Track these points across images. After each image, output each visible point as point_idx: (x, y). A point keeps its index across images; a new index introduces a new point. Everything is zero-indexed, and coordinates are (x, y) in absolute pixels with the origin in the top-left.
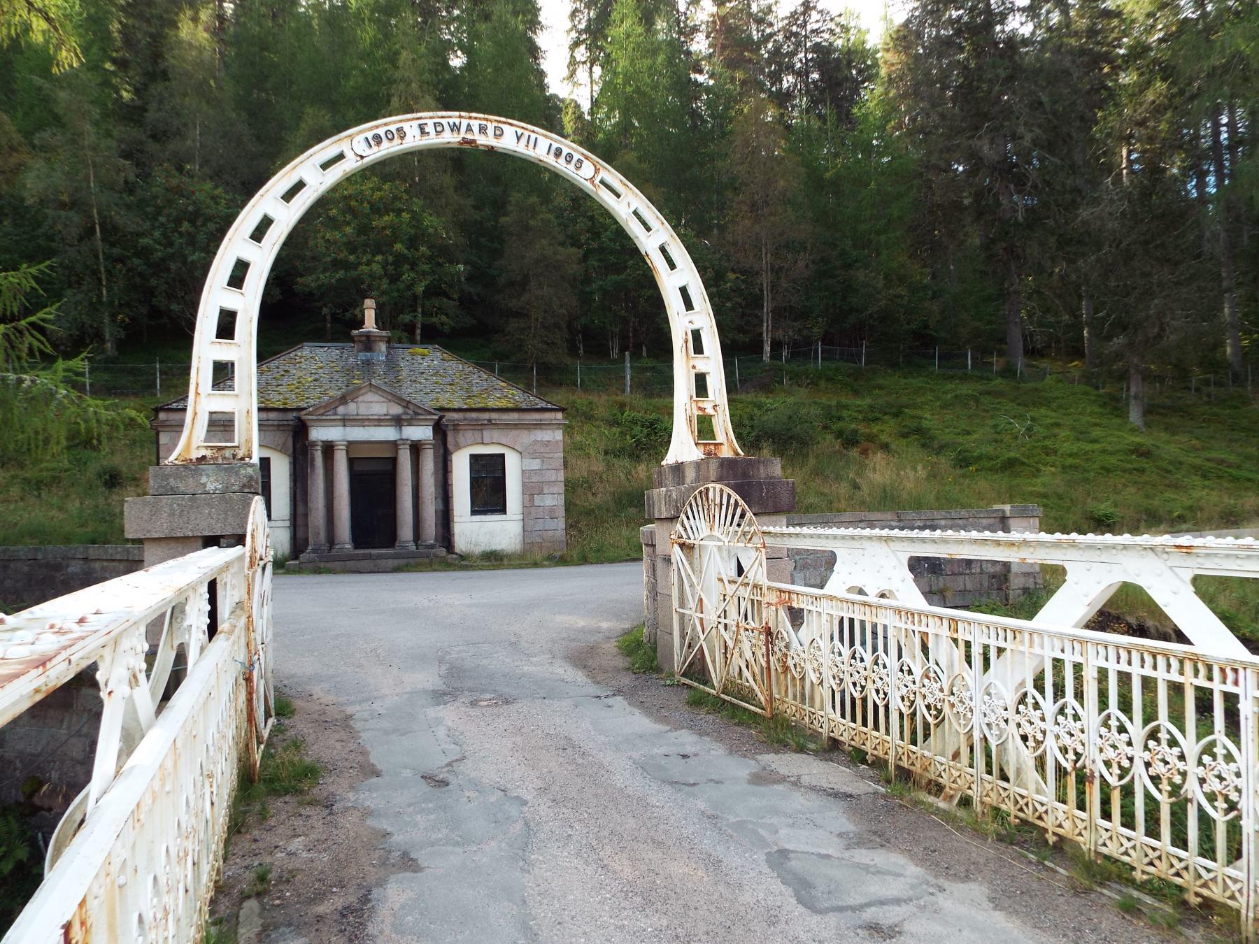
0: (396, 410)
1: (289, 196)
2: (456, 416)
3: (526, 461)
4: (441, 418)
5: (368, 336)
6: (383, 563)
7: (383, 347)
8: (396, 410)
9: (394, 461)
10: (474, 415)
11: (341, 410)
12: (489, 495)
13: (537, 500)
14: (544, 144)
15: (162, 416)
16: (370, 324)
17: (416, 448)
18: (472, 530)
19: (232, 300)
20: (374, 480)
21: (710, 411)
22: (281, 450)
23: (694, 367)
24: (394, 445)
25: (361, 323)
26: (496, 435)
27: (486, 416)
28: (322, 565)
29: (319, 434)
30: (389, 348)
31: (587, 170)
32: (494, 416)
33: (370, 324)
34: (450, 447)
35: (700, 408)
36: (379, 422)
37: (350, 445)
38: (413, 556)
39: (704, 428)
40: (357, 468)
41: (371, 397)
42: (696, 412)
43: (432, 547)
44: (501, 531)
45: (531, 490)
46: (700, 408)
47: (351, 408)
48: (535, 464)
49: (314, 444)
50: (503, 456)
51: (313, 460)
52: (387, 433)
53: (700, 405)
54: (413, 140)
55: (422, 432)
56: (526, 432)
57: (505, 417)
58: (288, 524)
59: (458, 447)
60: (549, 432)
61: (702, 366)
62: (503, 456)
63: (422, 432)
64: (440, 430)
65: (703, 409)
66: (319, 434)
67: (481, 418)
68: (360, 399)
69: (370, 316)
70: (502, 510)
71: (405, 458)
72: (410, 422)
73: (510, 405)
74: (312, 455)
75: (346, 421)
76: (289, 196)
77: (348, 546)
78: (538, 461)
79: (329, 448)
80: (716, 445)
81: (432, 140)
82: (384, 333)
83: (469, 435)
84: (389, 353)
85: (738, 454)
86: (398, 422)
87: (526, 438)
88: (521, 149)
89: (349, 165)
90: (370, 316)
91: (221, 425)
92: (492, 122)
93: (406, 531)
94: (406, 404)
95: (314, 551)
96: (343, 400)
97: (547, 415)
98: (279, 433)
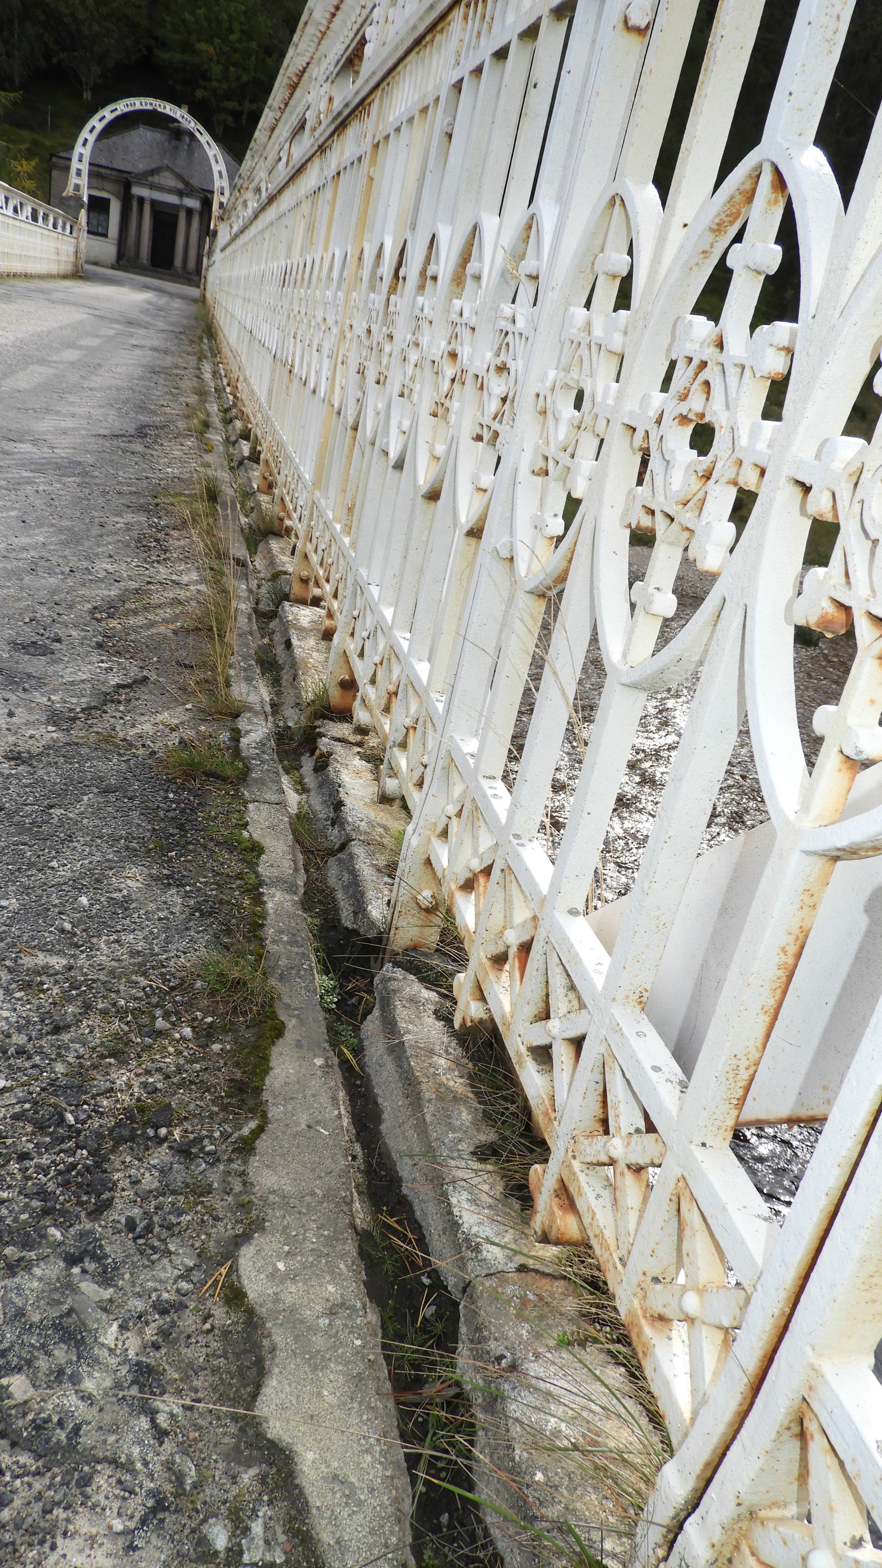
0: (180, 186)
1: (101, 120)
8: (180, 186)
9: (176, 218)
11: (150, 179)
14: (179, 113)
15: (54, 159)
17: (190, 212)
19: (83, 151)
22: (117, 197)
24: (177, 207)
31: (192, 124)
36: (170, 191)
37: (153, 202)
41: (167, 174)
47: (156, 179)
52: (173, 199)
54: (138, 107)
63: (193, 203)
66: (137, 191)
72: (188, 196)
75: (152, 187)
76: (101, 120)
79: (141, 200)
81: (144, 107)
86: (181, 194)
88: (171, 114)
89: (118, 113)
91: (77, 187)
92: (163, 103)
93: (178, 261)
94: (187, 184)
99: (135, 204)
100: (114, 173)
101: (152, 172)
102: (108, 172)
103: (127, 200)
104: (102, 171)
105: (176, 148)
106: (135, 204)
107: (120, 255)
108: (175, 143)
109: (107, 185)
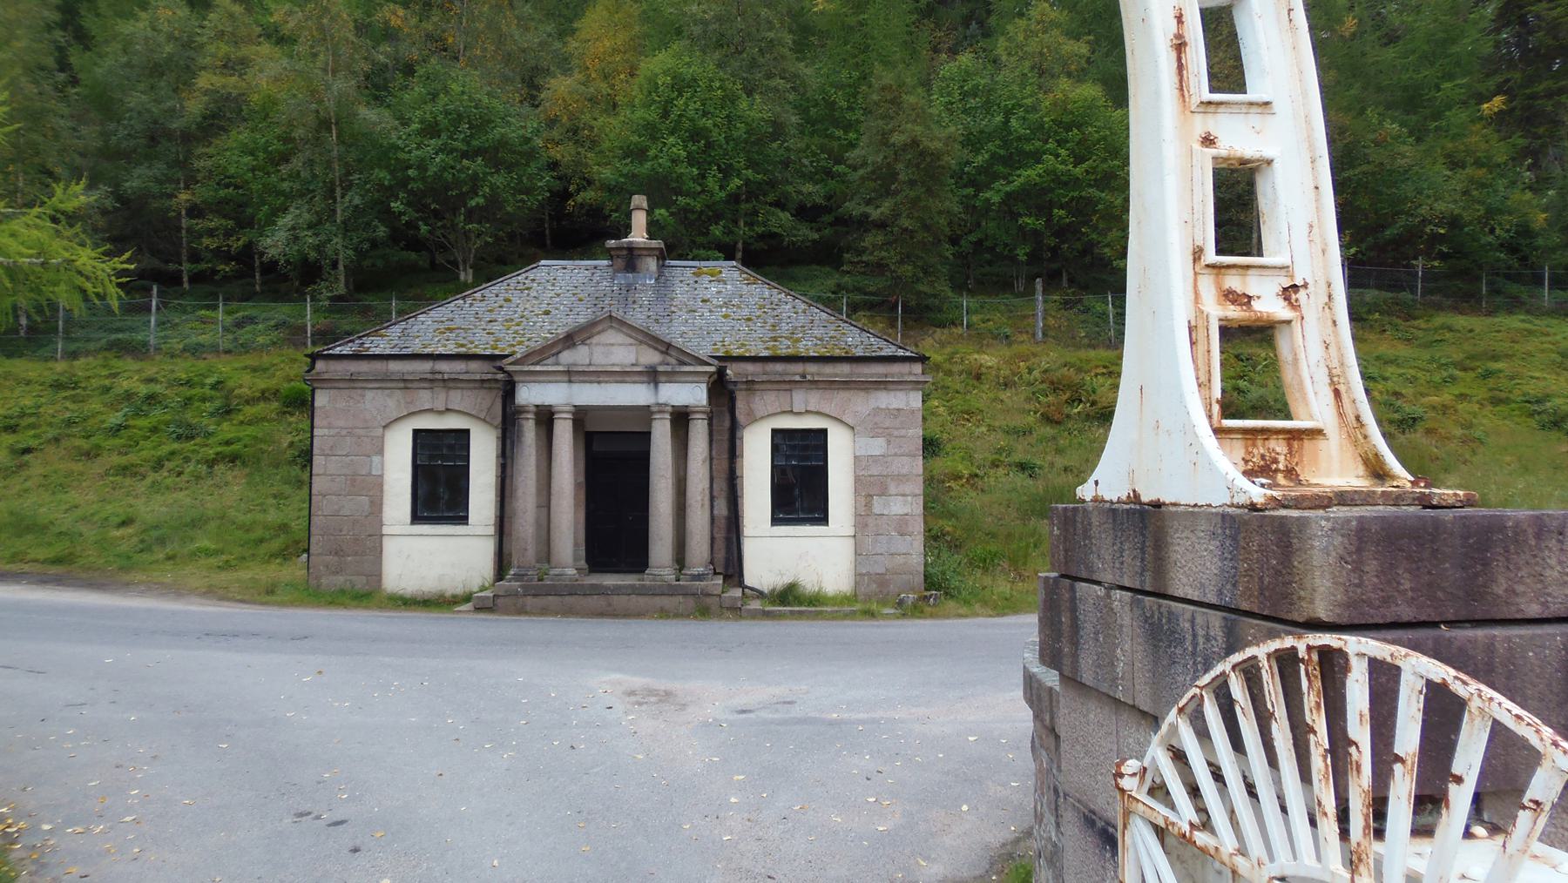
0: (651, 357)
2: (750, 368)
3: (862, 441)
4: (721, 372)
5: (631, 250)
6: (619, 601)
7: (652, 264)
8: (651, 357)
10: (779, 367)
11: (567, 357)
12: (801, 491)
13: (878, 505)
16: (638, 235)
17: (681, 418)
18: (775, 553)
20: (615, 463)
21: (1270, 305)
23: (1208, 141)
24: (645, 413)
25: (627, 229)
26: (814, 399)
27: (798, 368)
28: (529, 600)
29: (530, 395)
30: (661, 267)
32: (812, 368)
33: (638, 235)
34: (741, 416)
35: (1230, 296)
36: (622, 376)
37: (581, 416)
38: (671, 591)
39: (1249, 365)
40: (596, 447)
41: (612, 336)
42: (1217, 311)
43: (699, 577)
44: (815, 556)
45: (868, 487)
46: (1230, 296)
47: (577, 356)
48: (877, 446)
49: (521, 410)
50: (824, 432)
51: (520, 434)
52: (634, 395)
53: (1233, 282)
55: (693, 394)
56: (862, 394)
57: (829, 370)
58: (491, 530)
59: (754, 419)
60: (901, 395)
61: (1239, 138)
62: (824, 432)
63: (693, 394)
64: (722, 390)
65: (1245, 300)
66: (530, 395)
67: (789, 368)
68: (595, 340)
69: (639, 220)
70: (823, 519)
71: (661, 434)
72: (672, 377)
73: (837, 352)
74: (520, 426)
75: (572, 375)
77: (571, 571)
78: (881, 441)
79: (546, 417)
80: (1294, 436)
82: (655, 243)
83: (766, 401)
84: (660, 274)
85: (1378, 471)
86: (653, 376)
87: (862, 405)
90: (639, 220)
94: (666, 348)
95: (518, 577)
96: (569, 340)
97: (896, 368)
98: (482, 393)
99: (529, 430)
100: (474, 365)
101: (569, 340)
102: (459, 366)
103: (508, 424)
104: (444, 366)
105: (629, 288)
106: (529, 430)
107: (502, 563)
108: (622, 279)
109: (457, 398)
